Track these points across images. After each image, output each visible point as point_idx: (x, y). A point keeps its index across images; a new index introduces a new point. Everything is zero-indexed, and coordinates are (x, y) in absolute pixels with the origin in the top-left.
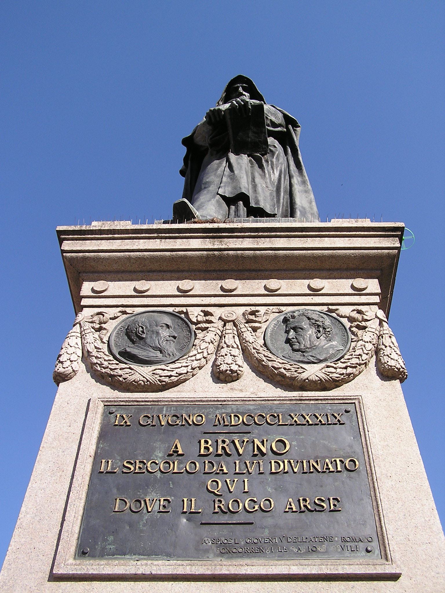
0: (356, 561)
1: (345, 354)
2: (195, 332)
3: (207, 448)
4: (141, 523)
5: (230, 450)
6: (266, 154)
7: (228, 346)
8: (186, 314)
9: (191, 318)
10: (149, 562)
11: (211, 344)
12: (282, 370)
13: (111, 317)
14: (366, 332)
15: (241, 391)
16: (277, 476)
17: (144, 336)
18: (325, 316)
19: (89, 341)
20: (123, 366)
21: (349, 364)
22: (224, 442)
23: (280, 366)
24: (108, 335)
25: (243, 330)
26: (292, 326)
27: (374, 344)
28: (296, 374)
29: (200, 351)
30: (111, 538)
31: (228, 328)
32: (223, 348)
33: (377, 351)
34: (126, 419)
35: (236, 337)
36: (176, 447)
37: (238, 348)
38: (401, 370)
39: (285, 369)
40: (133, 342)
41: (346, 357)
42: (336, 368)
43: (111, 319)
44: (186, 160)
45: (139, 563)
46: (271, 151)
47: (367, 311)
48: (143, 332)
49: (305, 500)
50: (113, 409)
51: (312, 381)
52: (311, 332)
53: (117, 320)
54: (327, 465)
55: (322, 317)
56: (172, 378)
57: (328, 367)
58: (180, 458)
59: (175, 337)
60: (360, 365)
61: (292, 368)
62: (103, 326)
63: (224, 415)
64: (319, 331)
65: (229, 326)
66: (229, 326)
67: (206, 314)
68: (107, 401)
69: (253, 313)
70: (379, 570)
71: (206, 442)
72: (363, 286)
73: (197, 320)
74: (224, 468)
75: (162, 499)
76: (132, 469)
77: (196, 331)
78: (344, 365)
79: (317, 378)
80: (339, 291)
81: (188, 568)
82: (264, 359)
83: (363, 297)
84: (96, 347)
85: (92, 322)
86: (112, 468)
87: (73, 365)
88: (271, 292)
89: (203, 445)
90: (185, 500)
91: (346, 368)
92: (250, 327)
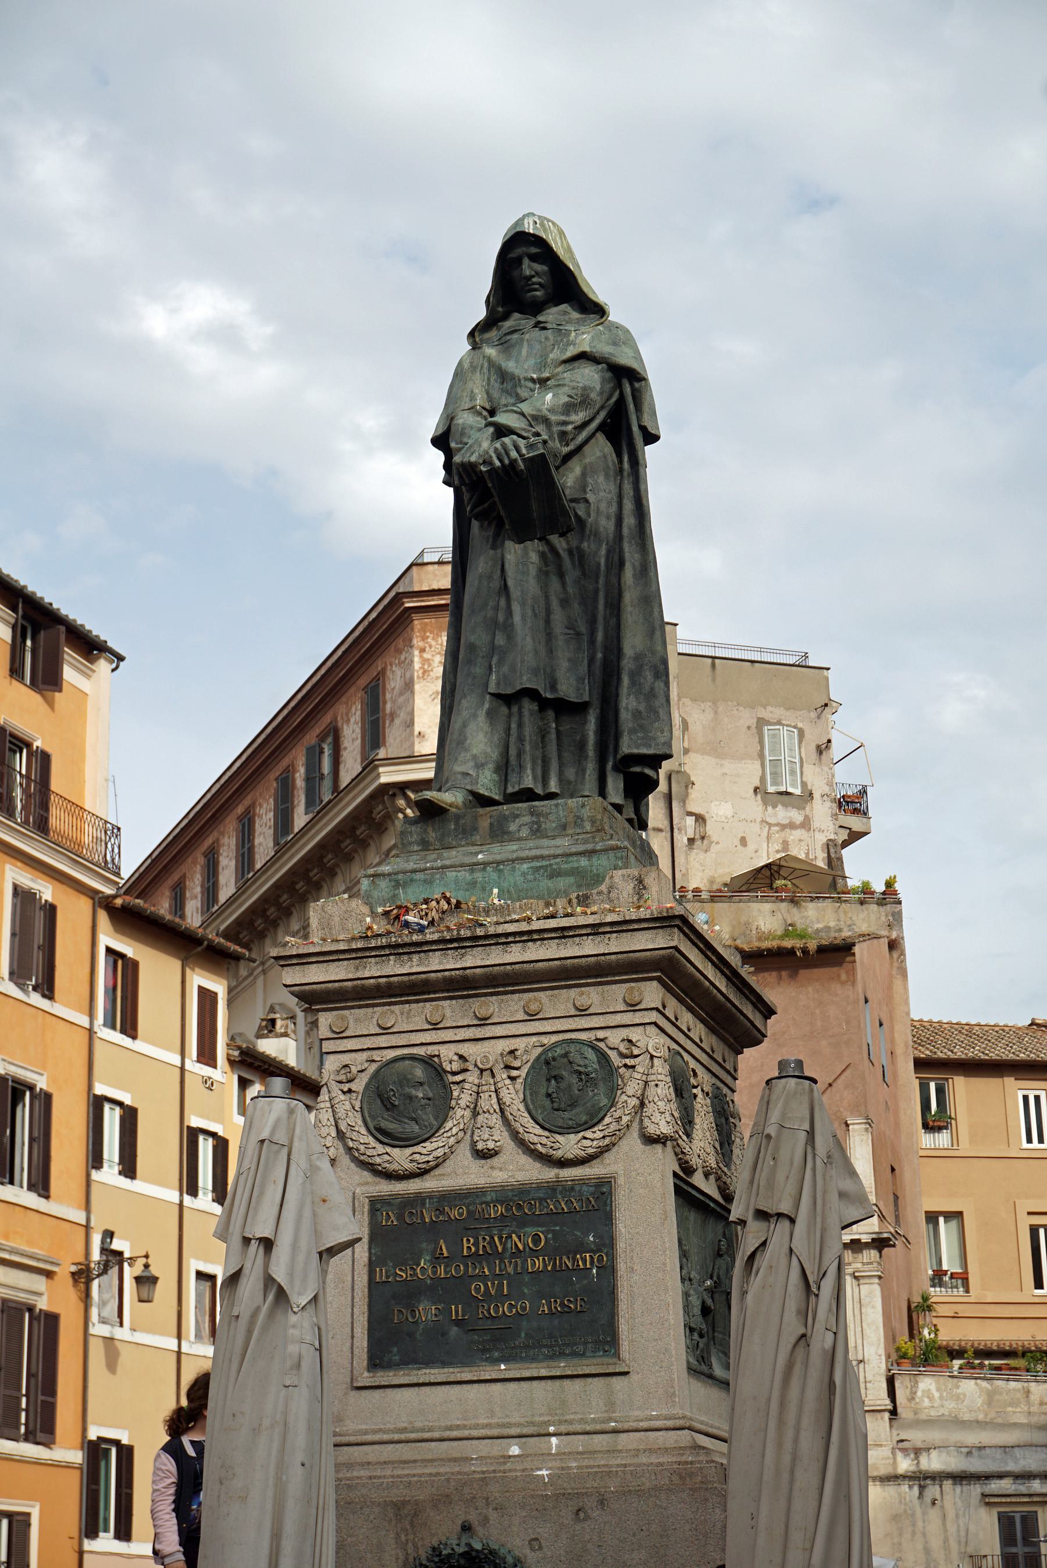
0: (595, 1361)
1: (605, 1115)
3: (469, 1248)
4: (418, 1333)
5: (491, 1248)
6: (570, 529)
7: (484, 1112)
8: (439, 1056)
10: (428, 1371)
11: (468, 1110)
12: (539, 1147)
15: (501, 1170)
16: (533, 1275)
17: (396, 1103)
18: (591, 1054)
19: (340, 1114)
20: (381, 1149)
21: (606, 1133)
22: (484, 1239)
23: (536, 1139)
24: (360, 1097)
26: (554, 1073)
27: (638, 1098)
28: (551, 1152)
29: (455, 1123)
30: (395, 1349)
32: (478, 1114)
33: (642, 1104)
34: (393, 1218)
35: (494, 1095)
36: (441, 1249)
37: (495, 1111)
38: (662, 1136)
39: (541, 1144)
40: (388, 1109)
41: (607, 1120)
42: (592, 1140)
43: (359, 1071)
45: (420, 1372)
46: (581, 522)
48: (394, 1095)
49: (555, 1301)
50: (378, 1206)
51: (567, 1160)
52: (574, 1080)
53: (366, 1072)
54: (578, 1262)
56: (431, 1163)
57: (585, 1138)
58: (446, 1260)
59: (429, 1099)
60: (619, 1130)
61: (549, 1143)
62: (353, 1086)
63: (484, 1206)
64: (581, 1080)
65: (486, 1074)
67: (461, 1057)
68: (371, 1197)
69: (512, 1052)
70: (611, 1370)
71: (468, 1240)
72: (637, 999)
74: (486, 1270)
75: (433, 1308)
76: (404, 1276)
78: (601, 1136)
79: (572, 1156)
81: (458, 1375)
82: (521, 1130)
83: (638, 1014)
84: (349, 1125)
85: (340, 1082)
86: (387, 1277)
87: (330, 1153)
88: (532, 1017)
89: (465, 1245)
90: (453, 1307)
91: (604, 1137)
92: (509, 1077)
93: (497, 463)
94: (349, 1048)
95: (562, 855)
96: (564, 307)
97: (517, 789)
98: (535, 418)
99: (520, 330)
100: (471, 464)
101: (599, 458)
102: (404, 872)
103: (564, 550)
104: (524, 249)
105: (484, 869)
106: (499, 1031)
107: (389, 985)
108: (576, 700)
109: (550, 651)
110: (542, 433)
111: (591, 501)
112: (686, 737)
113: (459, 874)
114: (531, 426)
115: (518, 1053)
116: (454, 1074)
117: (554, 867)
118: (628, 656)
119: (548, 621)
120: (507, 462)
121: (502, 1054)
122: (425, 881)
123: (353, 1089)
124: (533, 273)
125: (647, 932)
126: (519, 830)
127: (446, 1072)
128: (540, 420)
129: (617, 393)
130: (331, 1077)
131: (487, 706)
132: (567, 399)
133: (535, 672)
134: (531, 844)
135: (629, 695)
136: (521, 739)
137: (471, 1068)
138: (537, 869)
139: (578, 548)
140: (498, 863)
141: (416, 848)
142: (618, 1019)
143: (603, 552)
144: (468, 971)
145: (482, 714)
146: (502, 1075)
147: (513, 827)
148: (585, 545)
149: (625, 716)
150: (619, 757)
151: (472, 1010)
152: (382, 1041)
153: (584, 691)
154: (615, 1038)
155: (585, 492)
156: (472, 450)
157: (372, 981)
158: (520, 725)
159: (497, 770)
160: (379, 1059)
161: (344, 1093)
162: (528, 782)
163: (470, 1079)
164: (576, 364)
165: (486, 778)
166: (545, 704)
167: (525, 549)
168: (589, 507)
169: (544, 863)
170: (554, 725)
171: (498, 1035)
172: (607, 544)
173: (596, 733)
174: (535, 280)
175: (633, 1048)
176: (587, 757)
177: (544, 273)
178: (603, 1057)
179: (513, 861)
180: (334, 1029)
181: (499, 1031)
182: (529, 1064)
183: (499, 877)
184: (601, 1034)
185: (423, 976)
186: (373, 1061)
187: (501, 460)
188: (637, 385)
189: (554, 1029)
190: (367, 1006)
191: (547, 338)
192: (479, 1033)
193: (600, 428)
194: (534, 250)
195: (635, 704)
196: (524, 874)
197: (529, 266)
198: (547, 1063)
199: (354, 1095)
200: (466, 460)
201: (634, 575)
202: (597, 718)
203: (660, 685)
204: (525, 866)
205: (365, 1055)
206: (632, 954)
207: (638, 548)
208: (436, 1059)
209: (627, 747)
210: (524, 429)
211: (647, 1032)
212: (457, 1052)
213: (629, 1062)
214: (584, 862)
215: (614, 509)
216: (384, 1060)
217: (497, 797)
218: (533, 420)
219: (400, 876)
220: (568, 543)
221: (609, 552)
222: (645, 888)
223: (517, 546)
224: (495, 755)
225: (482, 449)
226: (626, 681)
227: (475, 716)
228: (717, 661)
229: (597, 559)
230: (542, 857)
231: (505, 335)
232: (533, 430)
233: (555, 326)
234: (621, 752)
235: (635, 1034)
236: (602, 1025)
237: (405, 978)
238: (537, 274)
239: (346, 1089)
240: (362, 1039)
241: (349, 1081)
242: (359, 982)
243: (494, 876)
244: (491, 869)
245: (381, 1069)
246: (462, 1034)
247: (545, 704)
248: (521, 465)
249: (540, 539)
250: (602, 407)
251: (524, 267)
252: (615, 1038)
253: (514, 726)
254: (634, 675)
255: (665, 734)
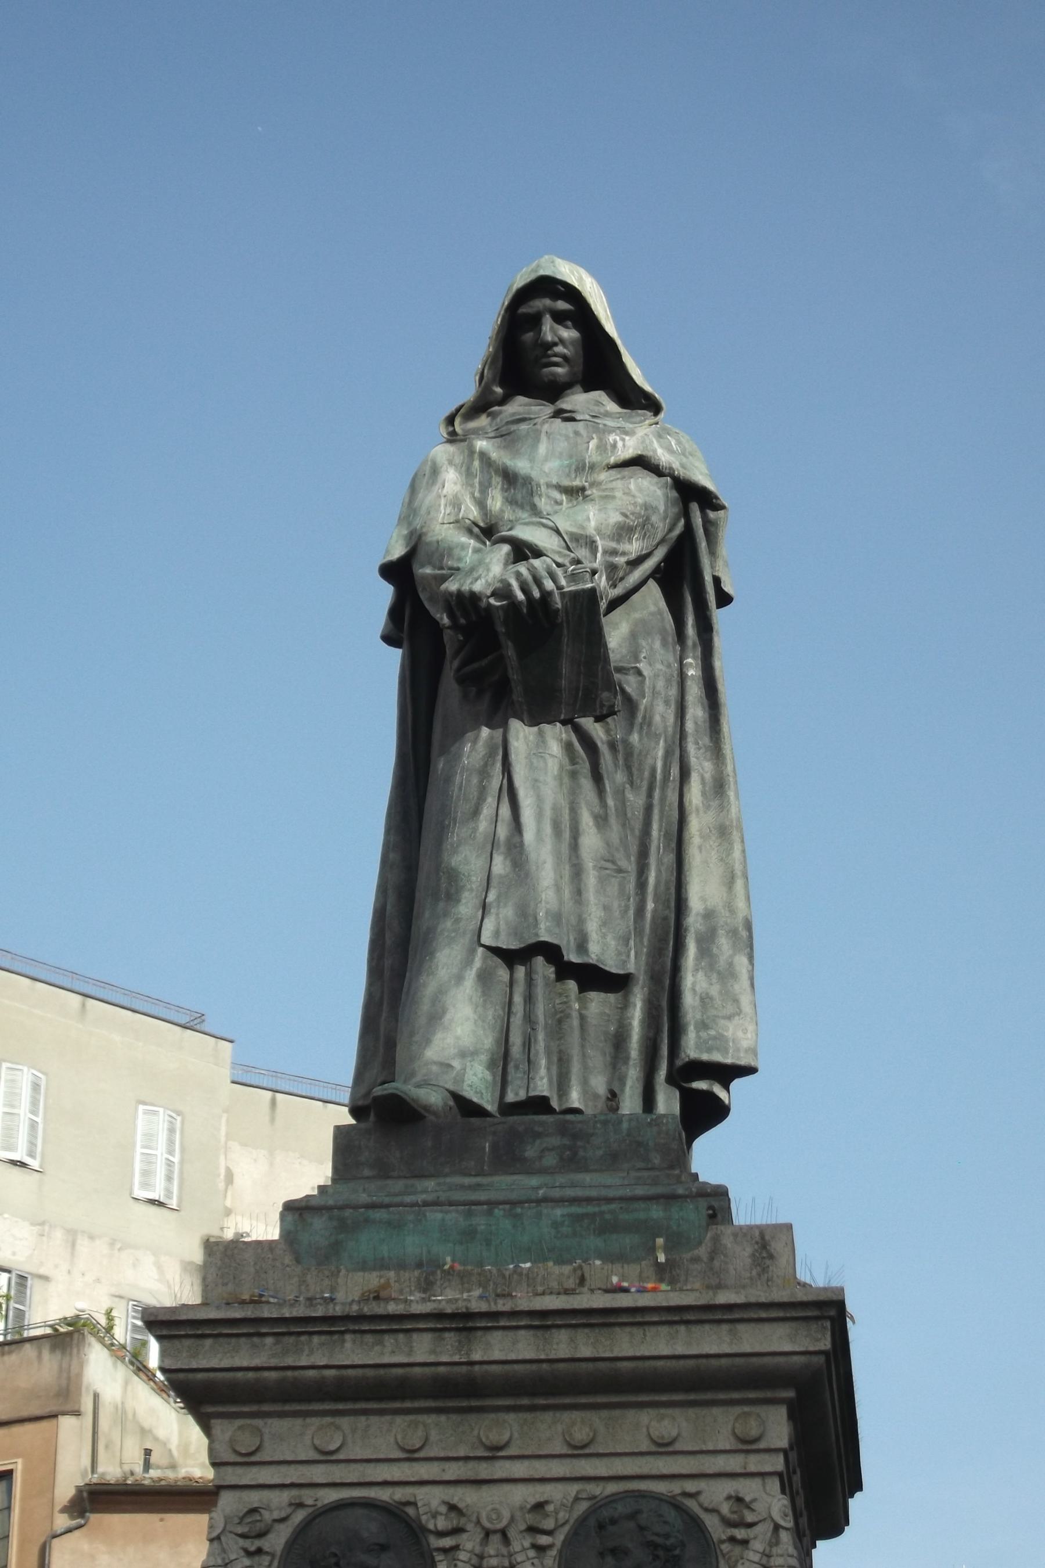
2: (433, 1558)
6: (612, 713)
8: (414, 1504)
9: (423, 1522)
13: (276, 1515)
14: (743, 1564)
18: (671, 1515)
25: (519, 1558)
31: (492, 1552)
43: (275, 1521)
44: (395, 613)
46: (628, 699)
47: (754, 1500)
55: (665, 1522)
62: (265, 1544)
65: (496, 1539)
66: (496, 1539)
67: (452, 1508)
72: (754, 1433)
73: (435, 1525)
77: (435, 1554)
80: (704, 1442)
85: (243, 1536)
88: (578, 1451)
92: (535, 1546)
93: (520, 596)
94: (261, 1481)
95: (622, 1199)
96: (600, 395)
97: (522, 1095)
98: (577, 538)
99: (531, 419)
100: (474, 598)
101: (652, 614)
102: (356, 1207)
103: (603, 743)
104: (547, 302)
105: (490, 1213)
106: (519, 1469)
107: (340, 1382)
108: (614, 970)
109: (578, 892)
110: (583, 560)
111: (645, 673)
112: (229, 1193)
113: (448, 1217)
114: (568, 549)
115: (550, 1508)
116: (441, 1534)
117: (608, 1216)
118: (694, 912)
119: (575, 846)
120: (536, 594)
121: (522, 1508)
122: (389, 1223)
123: (266, 1548)
124: (556, 339)
125: (781, 1324)
126: (540, 1158)
127: (425, 1530)
128: (582, 541)
129: (682, 522)
130: (228, 1528)
131: (478, 963)
132: (621, 519)
133: (557, 918)
134: (560, 1179)
135: (697, 970)
136: (529, 1019)
137: (470, 1527)
138: (578, 1218)
139: (625, 742)
140: (513, 1203)
141: (367, 1172)
142: (720, 1463)
143: (661, 753)
144: (477, 1368)
145: (471, 975)
146: (520, 1543)
147: (530, 1152)
148: (635, 738)
149: (689, 1000)
150: (679, 1063)
151: (475, 1433)
152: (318, 1474)
153: (628, 956)
154: (716, 1493)
155: (637, 660)
156: (475, 575)
157: (311, 1373)
158: (529, 999)
159: (491, 1065)
160: (310, 1502)
161: (249, 1554)
162: (542, 1086)
163: (469, 1546)
164: (627, 471)
165: (475, 1075)
166: (565, 970)
167: (541, 734)
168: (642, 682)
169: (591, 1209)
170: (577, 1006)
171: (517, 1476)
172: (666, 741)
173: (642, 1022)
174: (559, 349)
175: (746, 1512)
176: (627, 1058)
177: (573, 342)
178: (695, 1525)
179: (539, 1201)
180: (238, 1448)
181: (519, 1469)
182: (567, 1528)
183: (514, 1226)
184: (690, 1486)
185: (400, 1371)
186: (300, 1505)
187: (525, 590)
188: (712, 515)
189: (611, 1473)
190: (295, 1414)
191: (577, 433)
192: (484, 1470)
193: (656, 574)
194: (562, 305)
195: (704, 985)
196: (556, 1225)
197: (552, 329)
198: (601, 1526)
199: (267, 1559)
200: (466, 588)
201: (704, 794)
202: (644, 1001)
203: (741, 962)
204: (559, 1212)
205: (286, 1496)
206: (754, 1360)
207: (709, 754)
208: (411, 1511)
209: (692, 1048)
210: (559, 553)
211: (768, 1488)
212: (447, 1498)
213: (740, 1533)
214: (656, 1212)
215: (673, 692)
216: (319, 1504)
217: (489, 1107)
218: (571, 540)
219: (348, 1213)
220: (608, 731)
221: (668, 754)
222: (771, 1257)
223: (526, 728)
224: (488, 1041)
225: (491, 575)
226: (692, 949)
227: (459, 979)
228: (278, 1095)
229: (649, 761)
230: (589, 1200)
231: (508, 423)
232: (572, 555)
233: (588, 417)
234: (683, 1055)
235: (749, 1489)
236: (694, 1471)
237: (370, 1373)
238: (562, 341)
239: (253, 1549)
240: (283, 1469)
241: (261, 1535)
242: (289, 1373)
243: (507, 1224)
244: (501, 1213)
245: (314, 1518)
246: (453, 1471)
247: (565, 970)
248: (558, 602)
249: (564, 723)
250: (662, 541)
251: (544, 328)
252: (716, 1493)
253: (518, 999)
254: (706, 941)
255: (749, 1035)
